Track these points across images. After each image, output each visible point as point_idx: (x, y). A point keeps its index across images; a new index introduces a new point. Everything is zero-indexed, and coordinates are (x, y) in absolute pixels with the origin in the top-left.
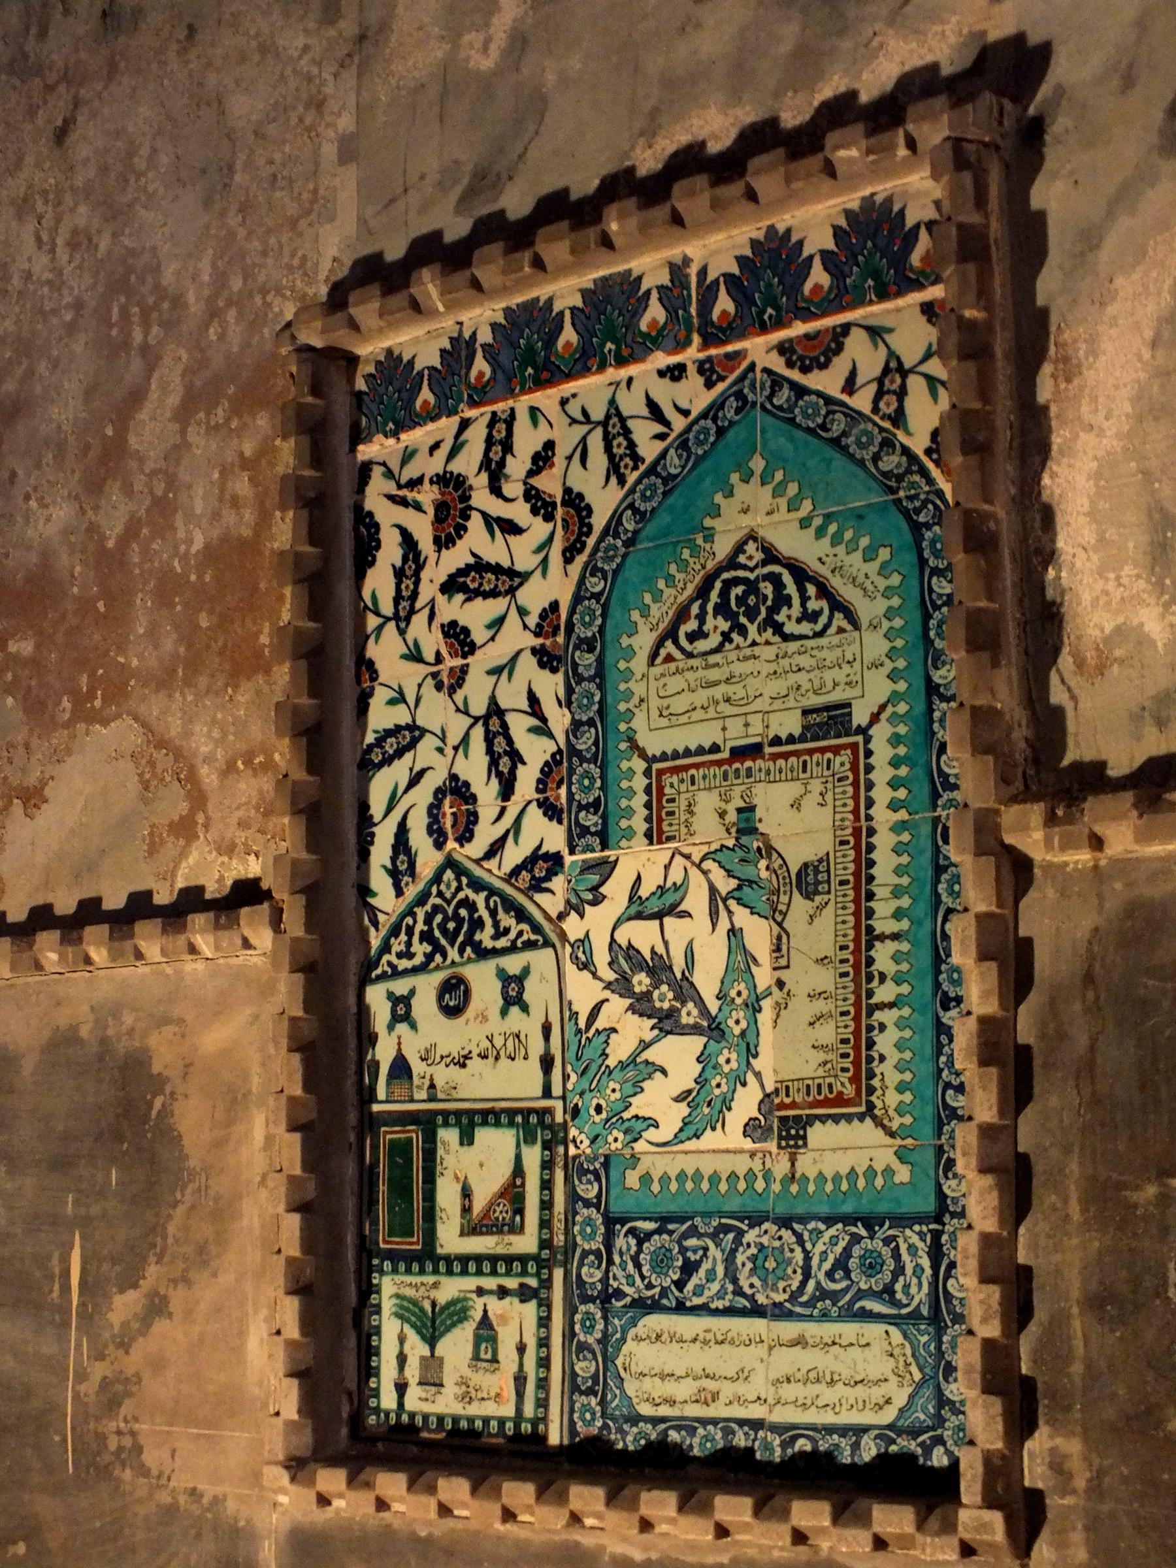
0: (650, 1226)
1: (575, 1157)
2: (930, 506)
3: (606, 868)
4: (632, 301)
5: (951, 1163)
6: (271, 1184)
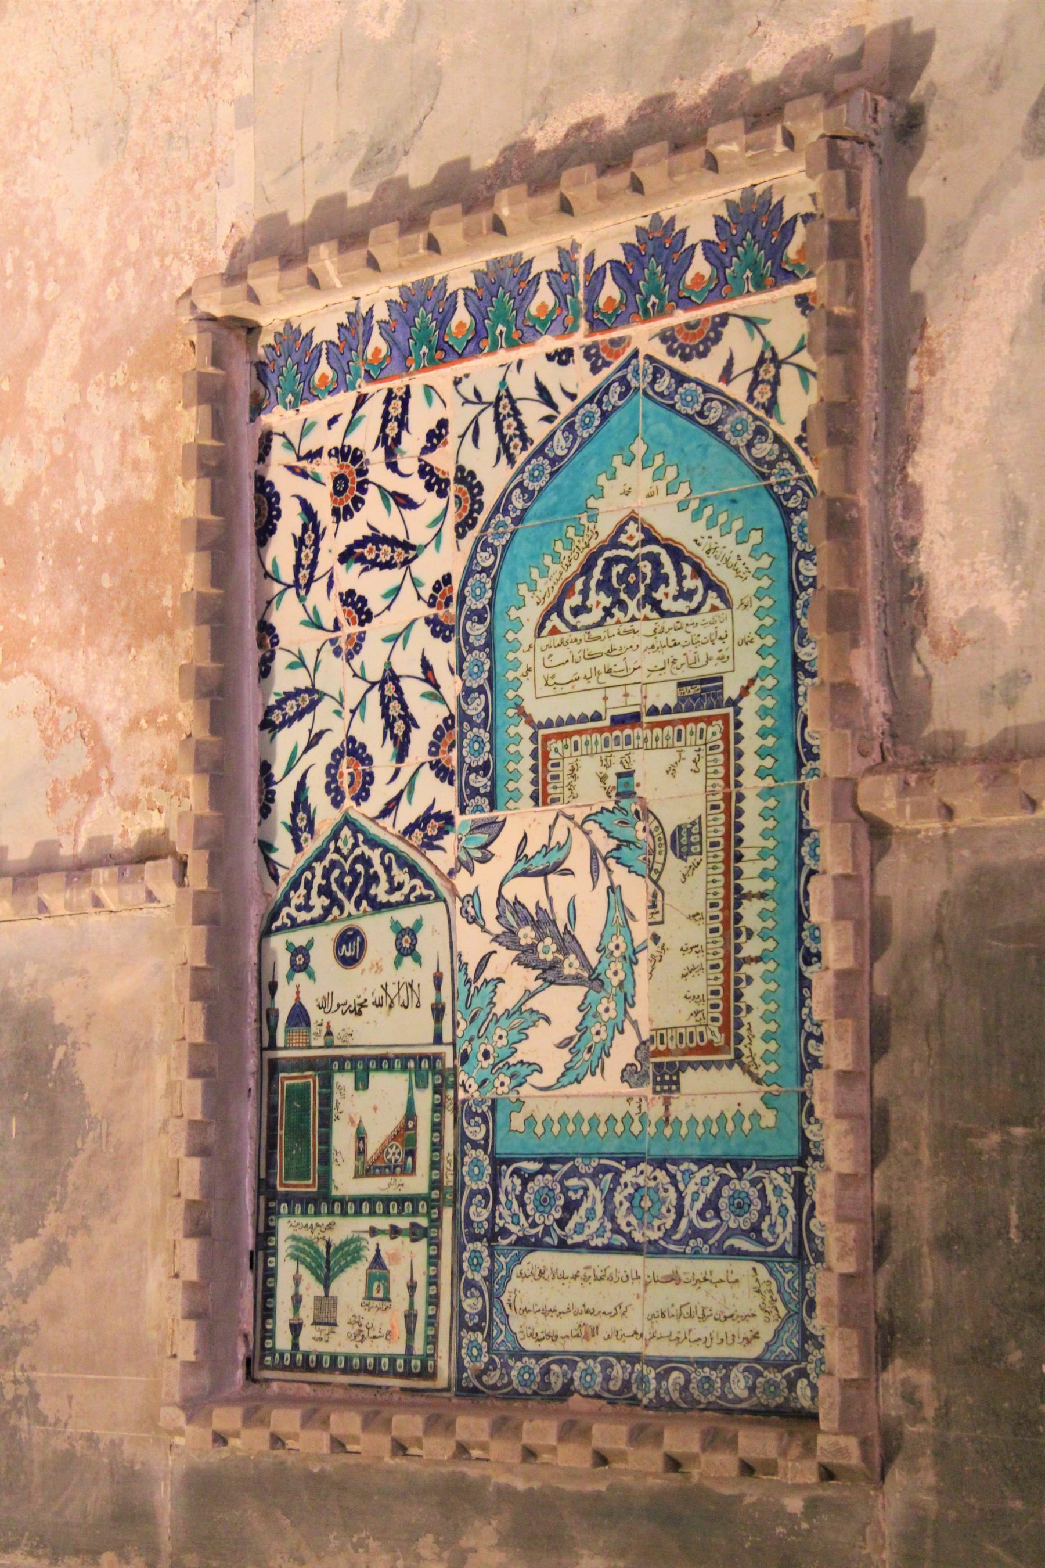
0: (534, 1166)
1: (464, 1101)
2: (799, 493)
3: (495, 828)
4: (523, 285)
6: (171, 1129)
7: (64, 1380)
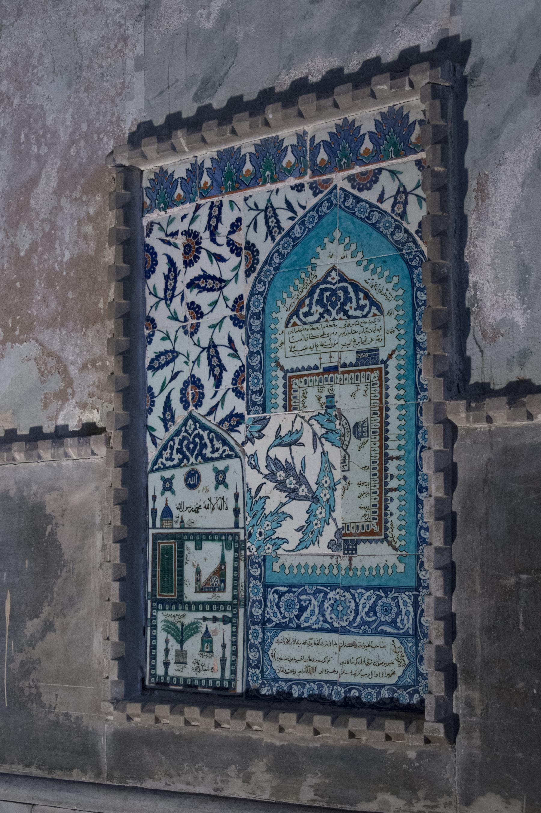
1: (249, 556)
2: (417, 258)
3: (265, 422)
4: (279, 151)
5: (422, 564)
6: (104, 567)
7: (54, 687)
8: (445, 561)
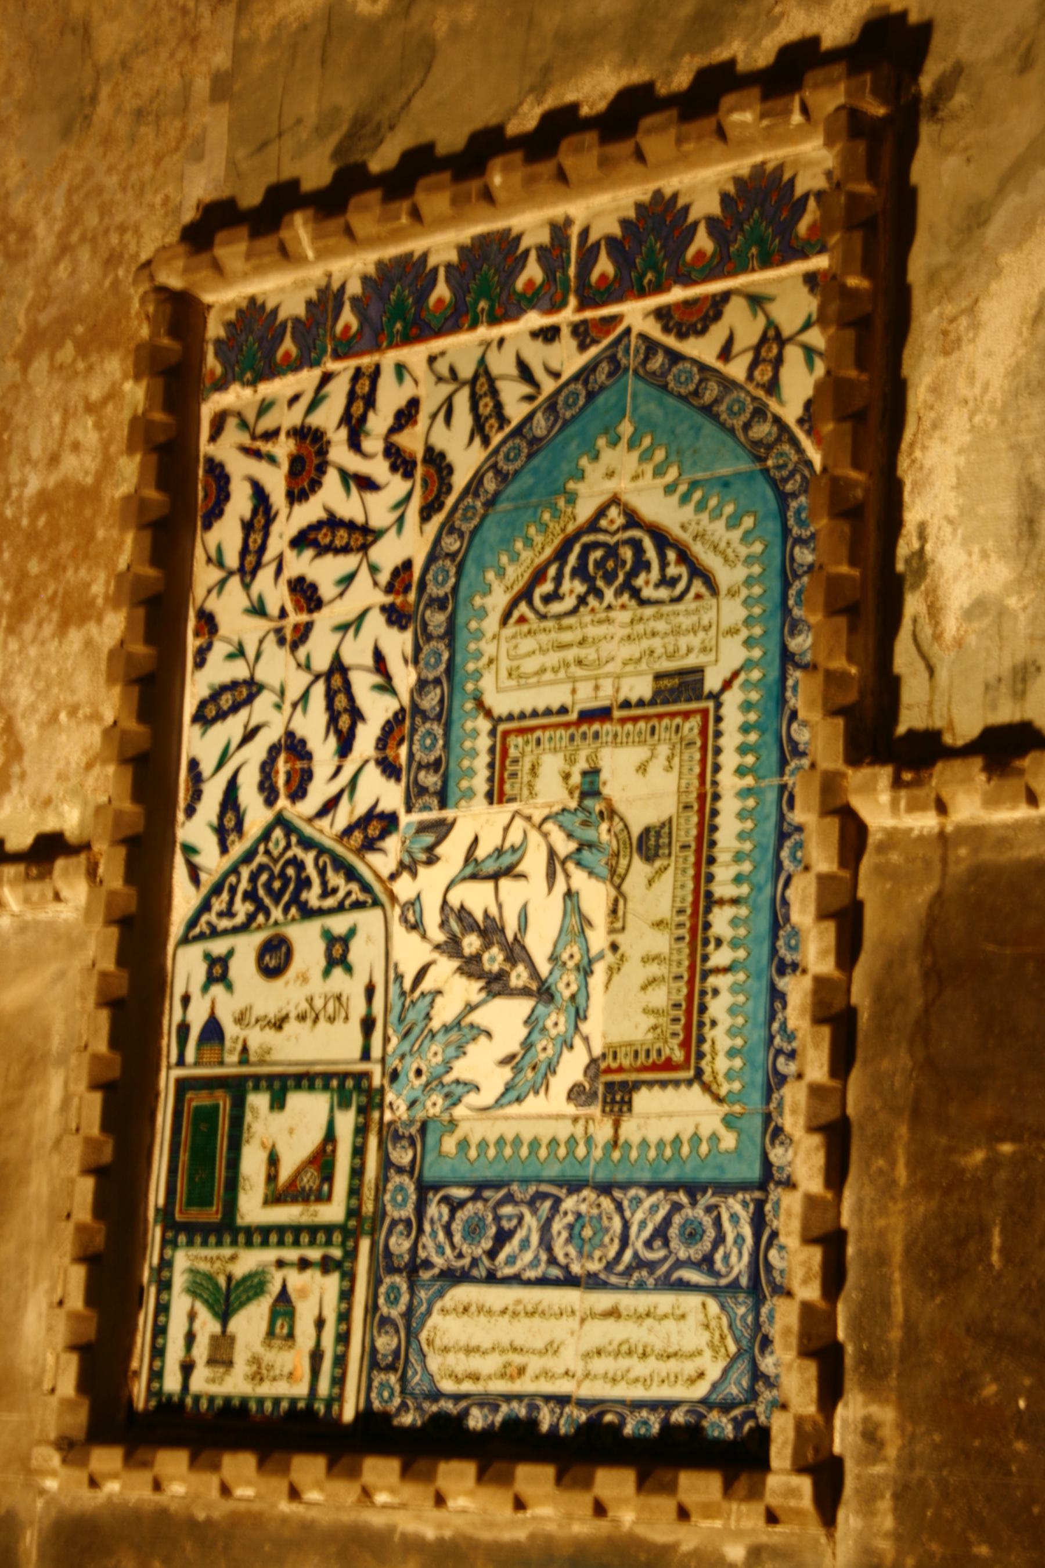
3: (442, 829)
6: (64, 1145)
8: (829, 1113)
